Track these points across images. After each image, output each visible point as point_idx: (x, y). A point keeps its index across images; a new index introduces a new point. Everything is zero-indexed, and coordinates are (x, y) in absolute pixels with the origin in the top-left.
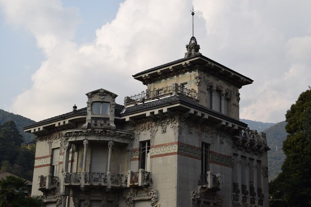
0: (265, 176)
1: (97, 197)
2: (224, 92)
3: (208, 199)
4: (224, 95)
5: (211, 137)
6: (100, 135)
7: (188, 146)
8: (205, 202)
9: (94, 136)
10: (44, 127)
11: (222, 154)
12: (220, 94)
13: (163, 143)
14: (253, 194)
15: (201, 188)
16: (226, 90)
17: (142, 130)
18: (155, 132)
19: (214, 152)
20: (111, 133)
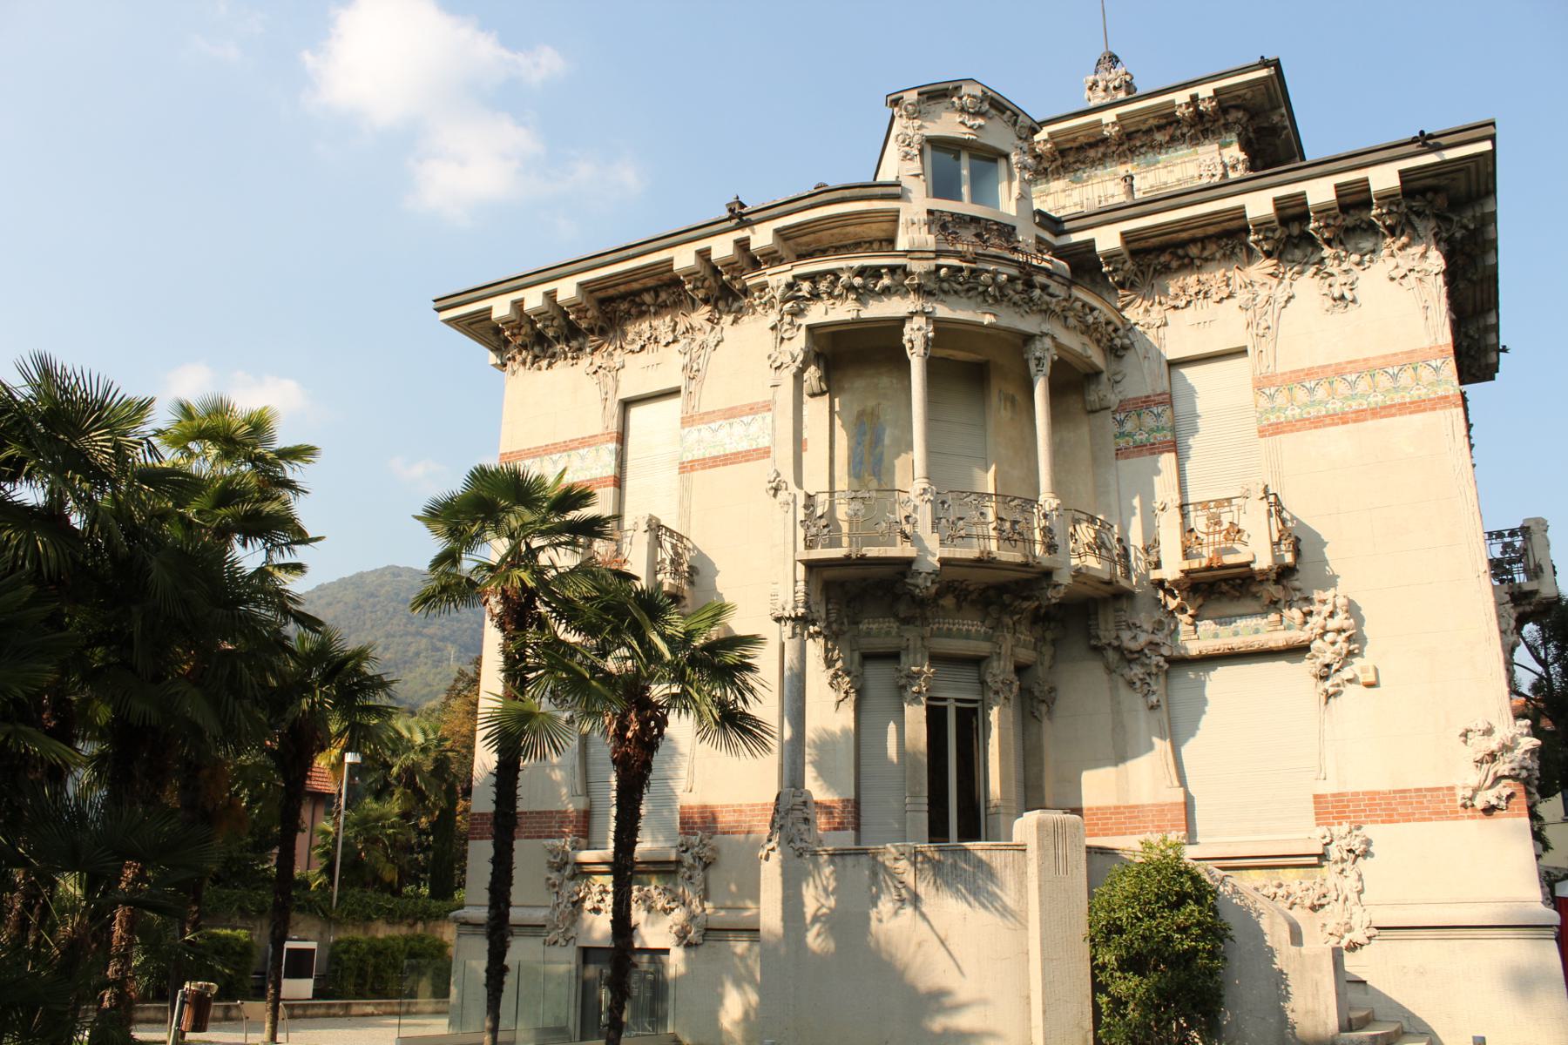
1: (967, 636)
6: (998, 296)
9: (965, 300)
10: (582, 286)
17: (1183, 303)
18: (1277, 306)
20: (1052, 295)
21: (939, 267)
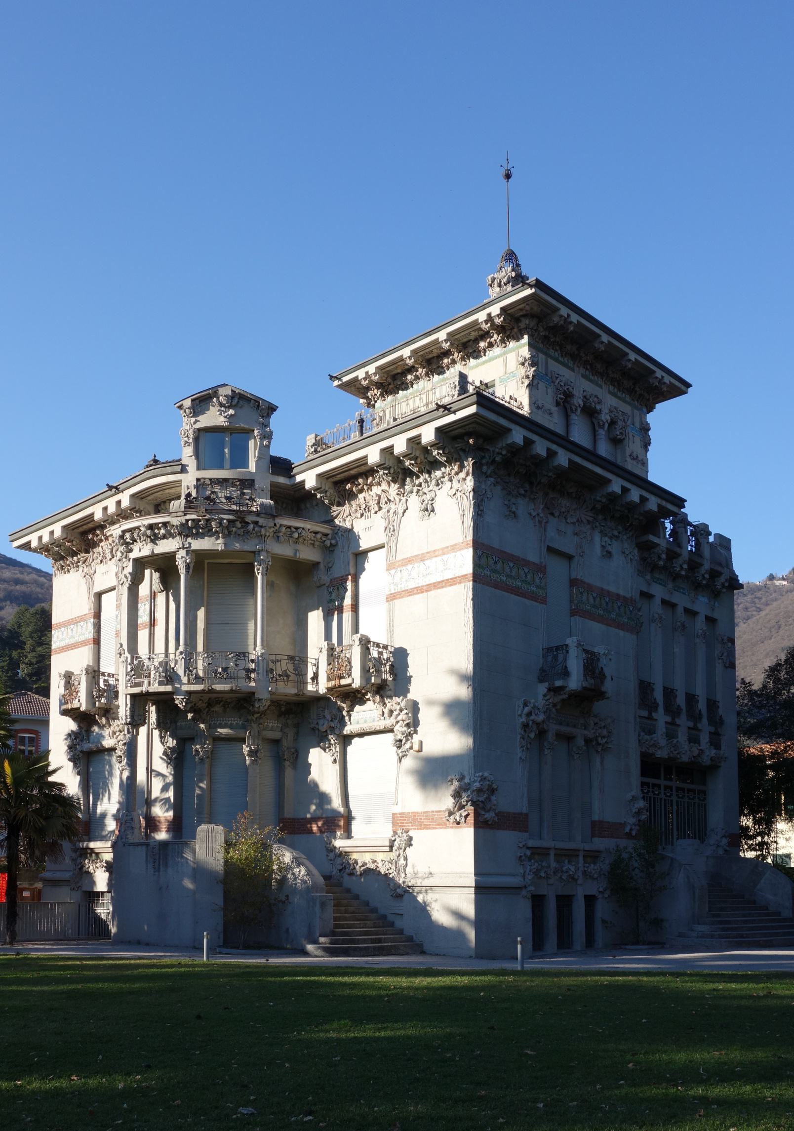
0: (727, 665)
2: (605, 417)
3: (568, 725)
4: (604, 425)
5: (576, 534)
7: (506, 557)
8: (559, 736)
10: (64, 528)
11: (608, 591)
12: (593, 424)
13: (425, 551)
14: (694, 716)
15: (549, 690)
16: (611, 411)
19: (584, 583)
21: (187, 521)
